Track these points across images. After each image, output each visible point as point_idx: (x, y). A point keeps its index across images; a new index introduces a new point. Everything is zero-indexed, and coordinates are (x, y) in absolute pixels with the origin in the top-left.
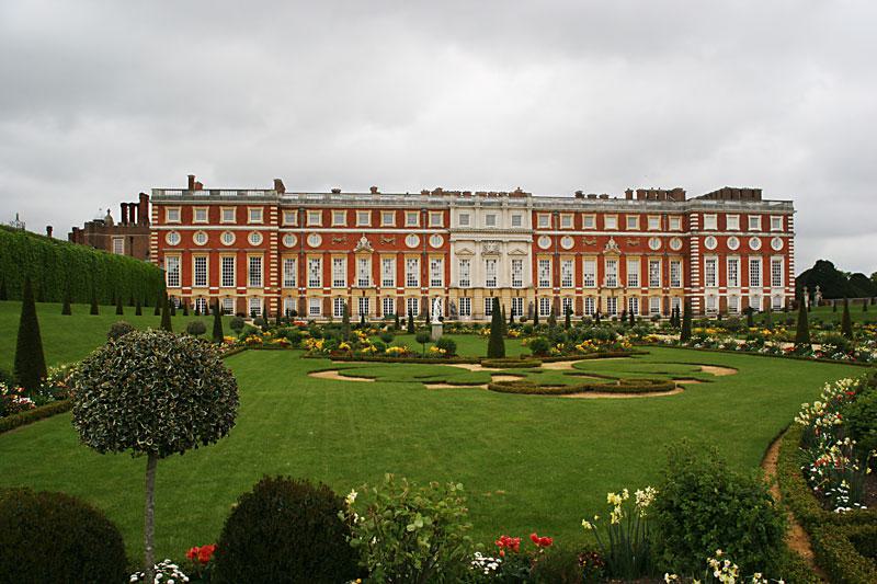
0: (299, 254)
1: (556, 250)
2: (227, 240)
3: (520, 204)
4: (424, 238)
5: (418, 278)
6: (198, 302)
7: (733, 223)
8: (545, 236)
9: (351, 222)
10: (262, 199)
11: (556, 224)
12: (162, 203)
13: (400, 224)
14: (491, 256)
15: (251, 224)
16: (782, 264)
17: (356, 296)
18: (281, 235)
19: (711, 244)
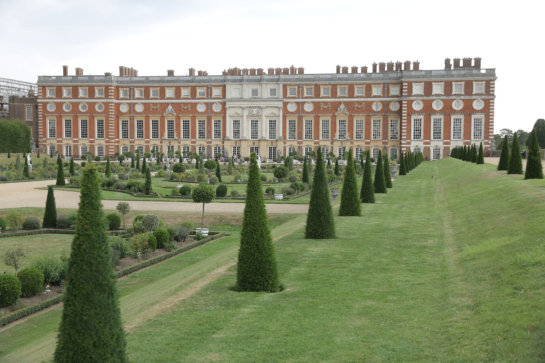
4: (209, 106)
9: (162, 94)
10: (104, 81)
16: (483, 121)
18: (118, 105)
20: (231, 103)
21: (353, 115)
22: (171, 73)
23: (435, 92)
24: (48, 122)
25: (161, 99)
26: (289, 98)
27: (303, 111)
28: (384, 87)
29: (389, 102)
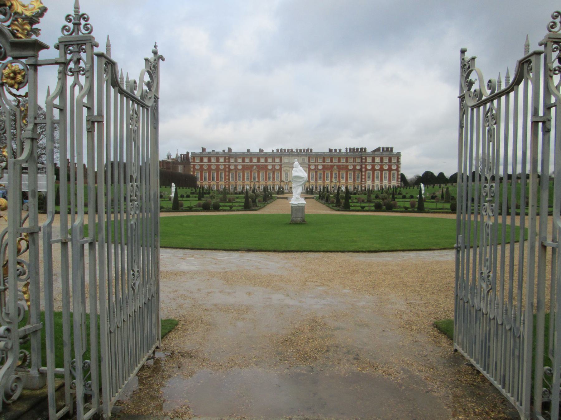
2: (213, 167)
7: (377, 160)
9: (251, 161)
11: (316, 161)
12: (194, 156)
18: (229, 165)
19: (369, 167)
22: (248, 150)
23: (376, 161)
27: (318, 169)
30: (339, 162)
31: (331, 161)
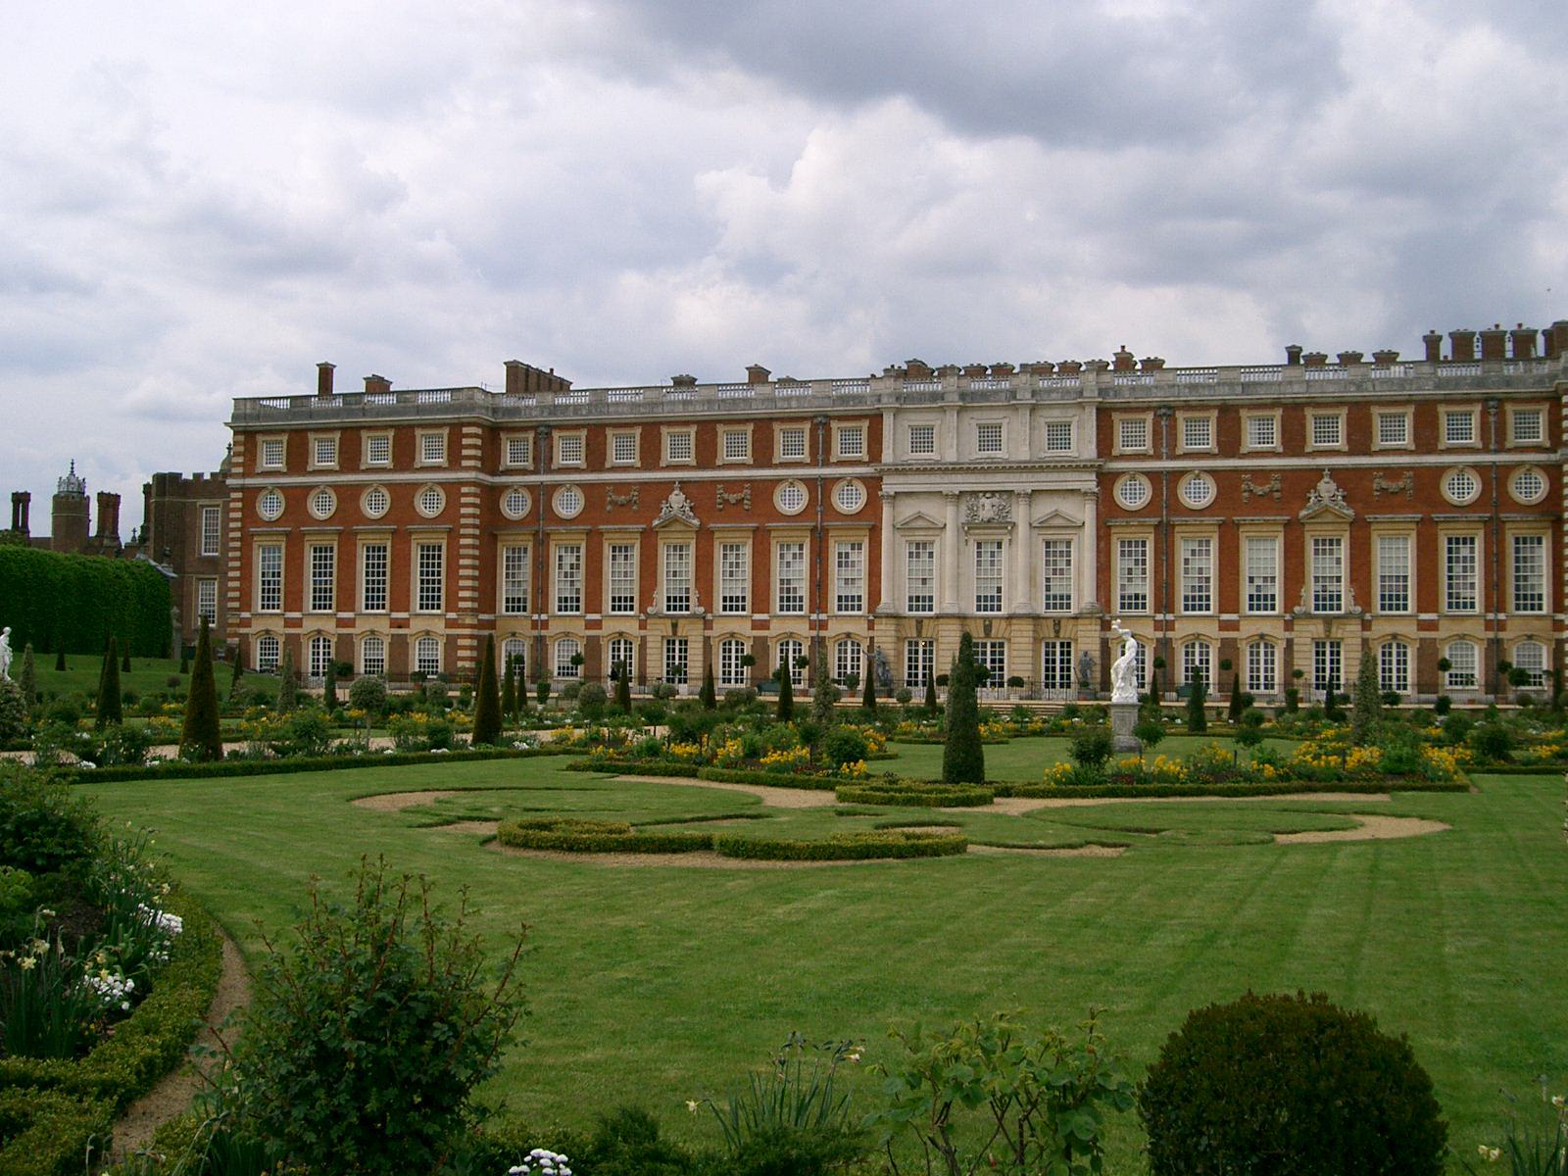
0: (536, 534)
1: (1165, 517)
3: (1067, 391)
4: (820, 489)
5: (803, 590)
6: (784, 653)
8: (1133, 475)
11: (1165, 441)
13: (763, 457)
14: (987, 533)
15: (614, 469)
17: (657, 633)
18: (491, 496)
20: (901, 479)
21: (1370, 517)
24: (258, 556)
25: (645, 468)
26: (1122, 457)
27: (1176, 507)
28: (1484, 414)
29: (1508, 469)
30: (1360, 442)
31: (1294, 442)
